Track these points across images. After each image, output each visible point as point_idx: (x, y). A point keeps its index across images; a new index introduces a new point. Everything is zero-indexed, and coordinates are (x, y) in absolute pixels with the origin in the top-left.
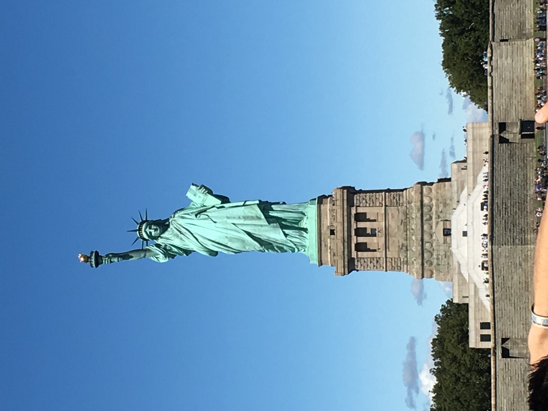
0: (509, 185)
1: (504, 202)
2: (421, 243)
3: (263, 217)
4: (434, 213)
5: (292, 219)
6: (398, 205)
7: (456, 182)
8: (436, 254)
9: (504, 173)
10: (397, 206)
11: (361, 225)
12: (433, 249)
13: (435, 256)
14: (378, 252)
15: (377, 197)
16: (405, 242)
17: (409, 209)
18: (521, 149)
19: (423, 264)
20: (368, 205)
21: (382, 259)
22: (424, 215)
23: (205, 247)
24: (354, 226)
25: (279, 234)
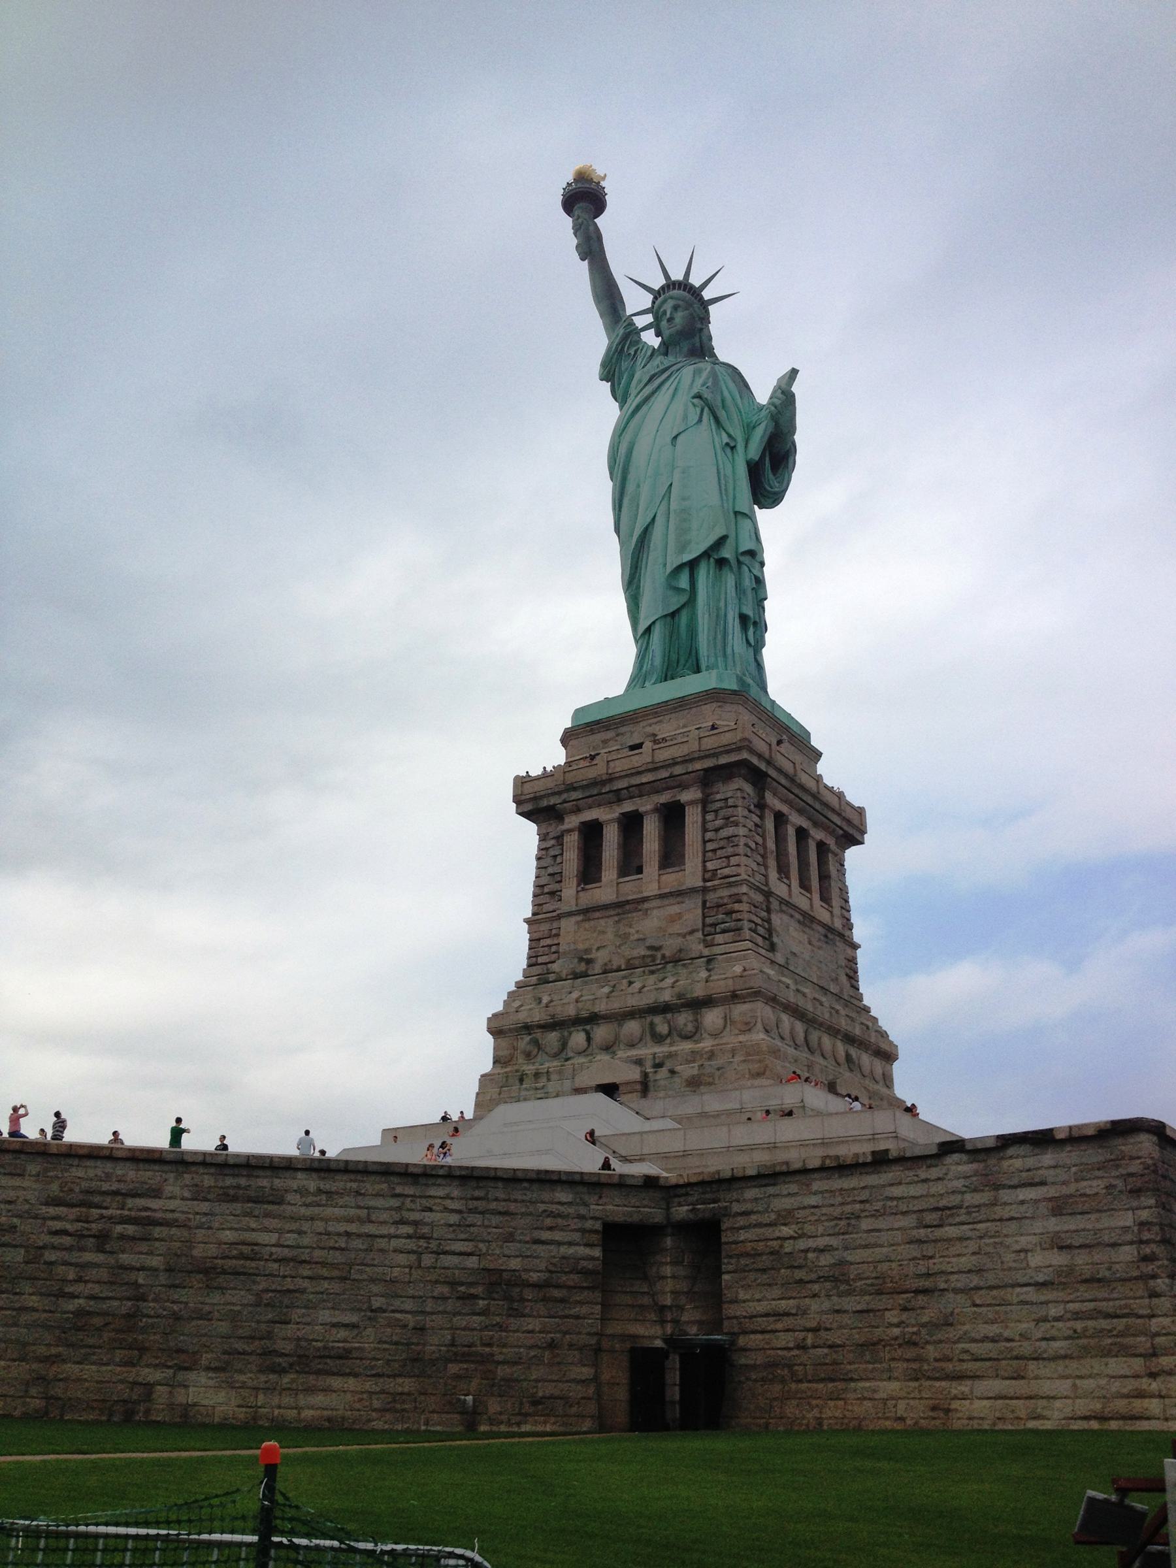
0: (285, 1270)
1: (157, 1231)
2: (585, 1014)
3: (687, 557)
4: (673, 1049)
7: (738, 1106)
9: (382, 1243)
10: (704, 925)
11: (651, 829)
12: (567, 1060)
14: (578, 892)
15: (733, 861)
16: (597, 968)
17: (691, 964)
18: (552, 1345)
19: (527, 1028)
20: (709, 835)
22: (669, 1016)
24: (645, 805)
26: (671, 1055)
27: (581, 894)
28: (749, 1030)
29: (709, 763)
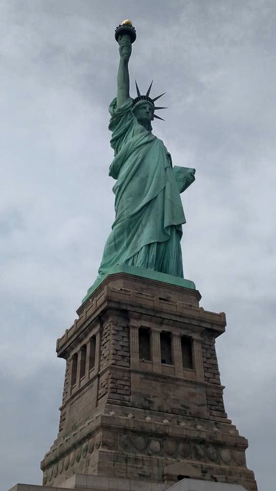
2: (161, 433)
3: (175, 224)
4: (207, 464)
5: (165, 262)
6: (209, 406)
8: (145, 459)
10: (208, 404)
11: (176, 344)
13: (140, 455)
16: (155, 407)
17: (208, 422)
19: (126, 430)
21: (127, 364)
22: (203, 446)
23: (134, 151)
25: (151, 238)
26: (211, 468)
27: (141, 363)
28: (242, 465)
29: (209, 326)
